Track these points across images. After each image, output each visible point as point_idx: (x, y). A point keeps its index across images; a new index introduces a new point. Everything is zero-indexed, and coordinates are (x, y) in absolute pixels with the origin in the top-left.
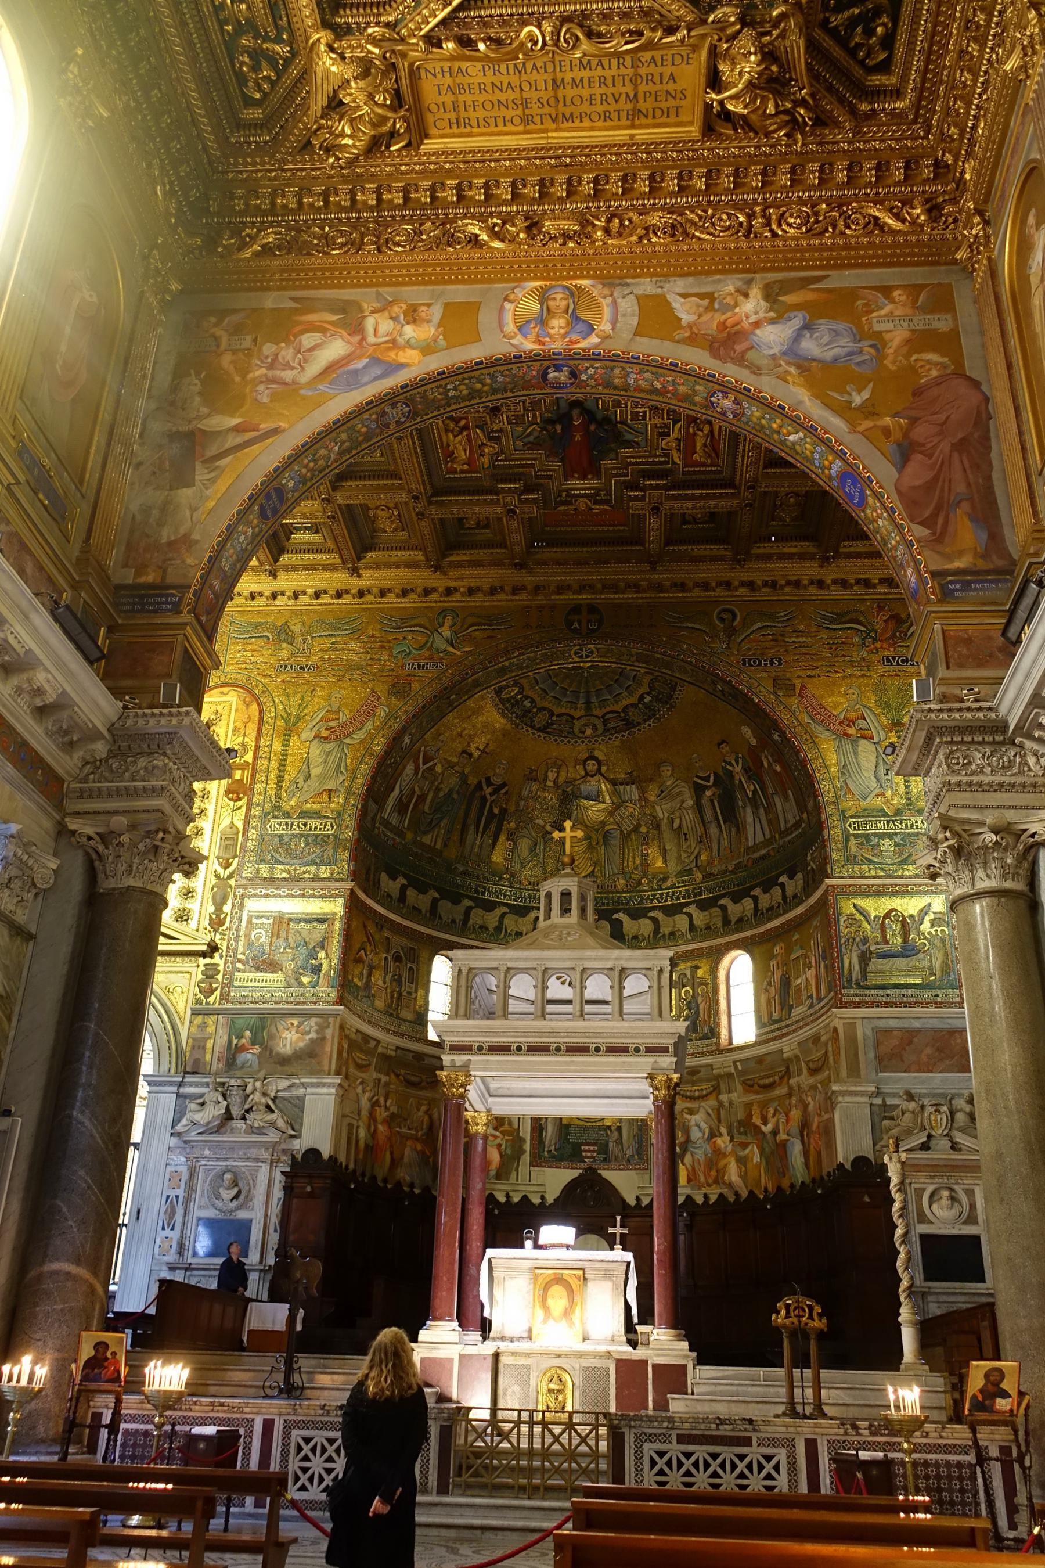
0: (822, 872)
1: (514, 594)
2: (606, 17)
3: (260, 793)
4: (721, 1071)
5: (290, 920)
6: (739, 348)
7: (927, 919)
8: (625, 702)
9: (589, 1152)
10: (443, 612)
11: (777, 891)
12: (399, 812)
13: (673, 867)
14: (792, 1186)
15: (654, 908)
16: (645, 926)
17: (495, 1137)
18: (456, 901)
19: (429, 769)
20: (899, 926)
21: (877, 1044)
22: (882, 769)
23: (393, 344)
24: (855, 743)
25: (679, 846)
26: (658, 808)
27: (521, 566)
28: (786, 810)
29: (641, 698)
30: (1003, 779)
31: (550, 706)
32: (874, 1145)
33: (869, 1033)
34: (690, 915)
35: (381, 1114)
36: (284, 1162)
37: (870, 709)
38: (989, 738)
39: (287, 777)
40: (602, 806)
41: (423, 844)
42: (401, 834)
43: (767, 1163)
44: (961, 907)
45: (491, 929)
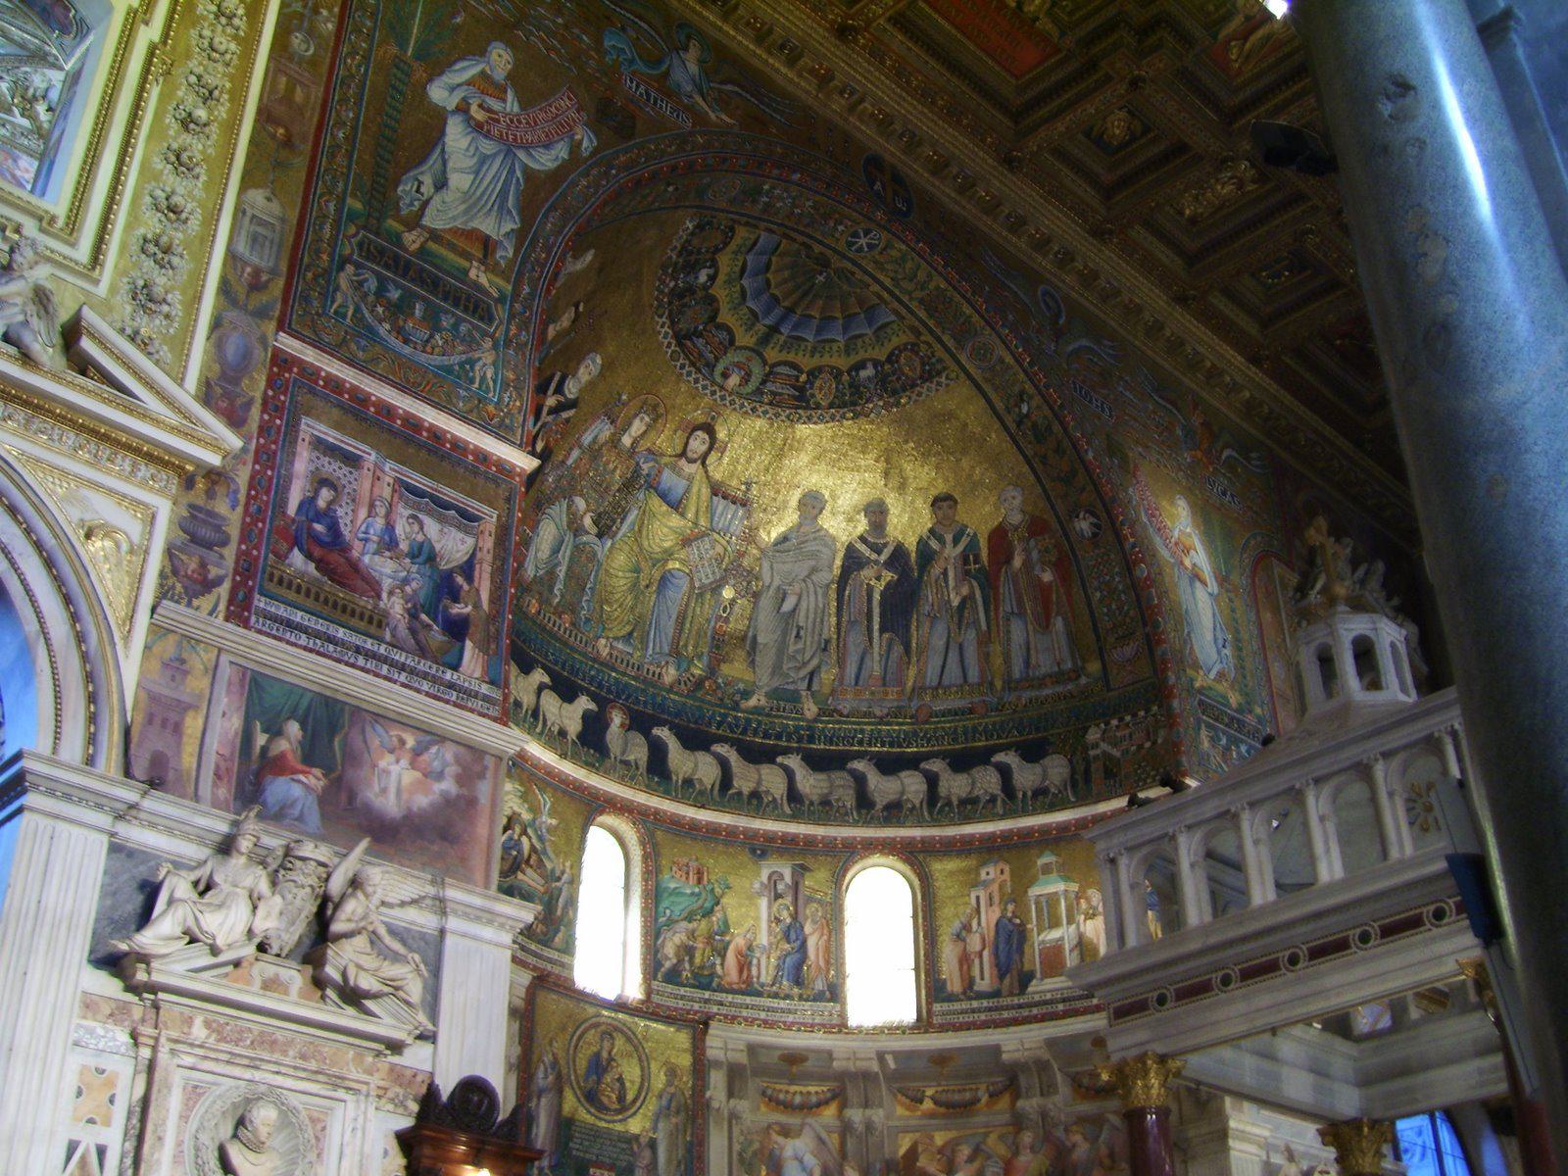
4: (851, 1067)
8: (826, 360)
13: (764, 679)
16: (704, 768)
26: (766, 565)
34: (790, 774)
40: (675, 521)
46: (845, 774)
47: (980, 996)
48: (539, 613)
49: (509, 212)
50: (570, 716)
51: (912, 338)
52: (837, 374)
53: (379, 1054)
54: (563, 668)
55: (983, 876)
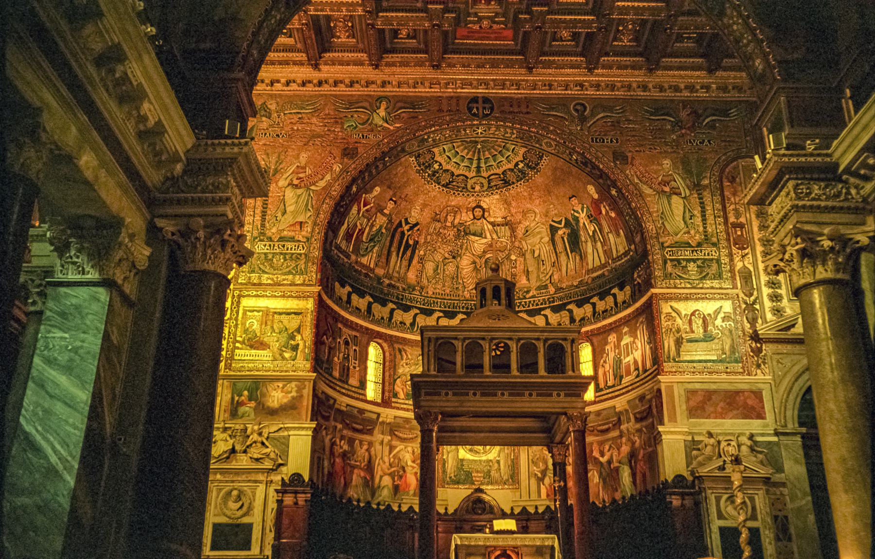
0: (648, 284)
1: (431, 88)
3: (249, 224)
5: (275, 313)
7: (722, 315)
8: (505, 168)
9: (477, 476)
10: (380, 99)
11: (610, 300)
12: (347, 240)
13: (534, 283)
14: (624, 498)
15: (521, 311)
17: (413, 467)
19: (367, 211)
20: (701, 320)
21: (688, 400)
22: (688, 215)
24: (669, 197)
25: (539, 269)
26: (524, 243)
27: (437, 67)
28: (618, 243)
29: (517, 165)
30: (835, 204)
31: (452, 169)
32: (688, 467)
33: (682, 393)
34: (546, 316)
36: (277, 483)
37: (679, 174)
38: (822, 176)
39: (269, 212)
40: (484, 241)
41: (361, 263)
43: (604, 483)
44: (804, 293)
45: (408, 325)
46: (566, 312)
47: (610, 387)
48: (434, 293)
49: (309, 210)
51: (523, 150)
52: (511, 170)
53: (268, 472)
54: (449, 308)
55: (609, 341)
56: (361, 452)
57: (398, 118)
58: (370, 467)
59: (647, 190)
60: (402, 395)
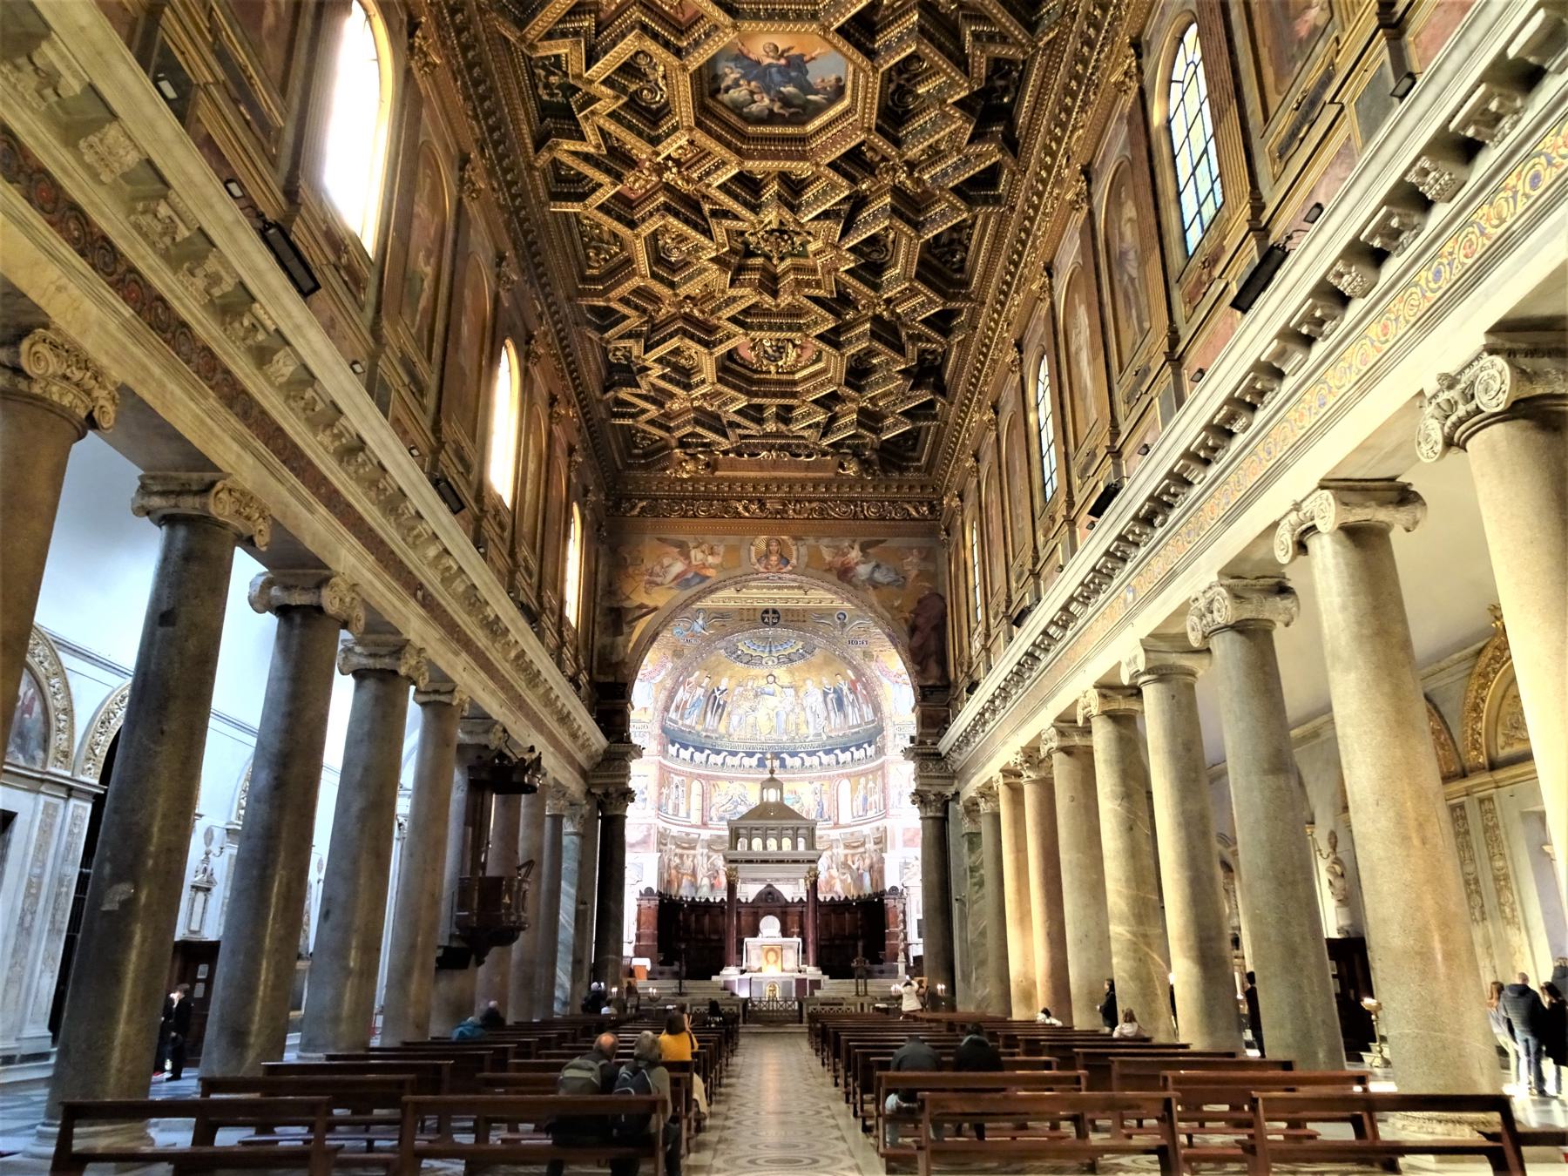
2: (798, 446)
6: (850, 575)
11: (862, 751)
13: (812, 731)
16: (797, 762)
18: (702, 752)
23: (704, 566)
28: (868, 713)
35: (673, 864)
42: (676, 723)
50: (754, 761)
56: (688, 863)
57: (712, 626)
58: (694, 874)
59: (885, 681)
60: (715, 819)
